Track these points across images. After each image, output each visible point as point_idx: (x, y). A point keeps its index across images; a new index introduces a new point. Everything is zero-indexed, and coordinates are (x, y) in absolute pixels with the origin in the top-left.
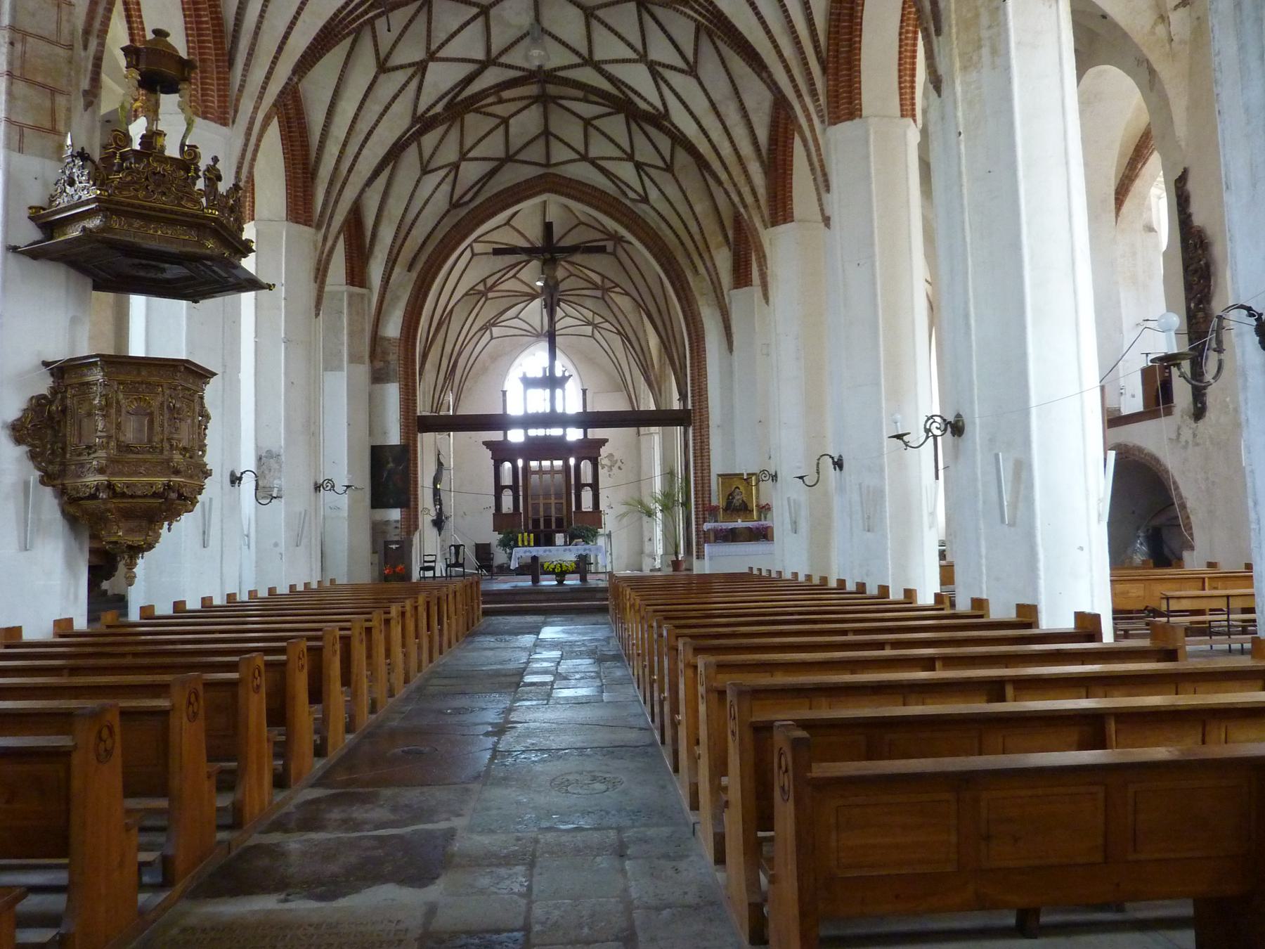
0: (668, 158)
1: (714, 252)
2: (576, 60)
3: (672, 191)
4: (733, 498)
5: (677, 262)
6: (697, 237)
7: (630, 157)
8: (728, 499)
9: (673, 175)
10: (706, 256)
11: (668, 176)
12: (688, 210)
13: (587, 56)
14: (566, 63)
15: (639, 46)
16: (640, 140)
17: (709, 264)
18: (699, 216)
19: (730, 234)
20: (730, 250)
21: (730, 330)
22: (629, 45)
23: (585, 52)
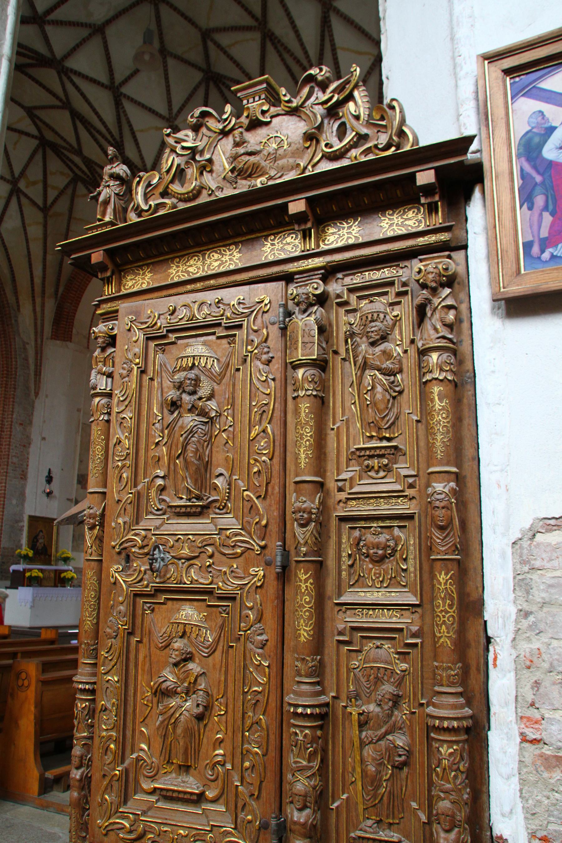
0: (50, 201)
1: (46, 300)
2: (104, 78)
3: (35, 231)
4: (37, 541)
5: (5, 294)
6: (38, 280)
7: (14, 182)
8: (33, 541)
9: (45, 217)
10: (38, 300)
11: (40, 216)
12: (41, 253)
13: (117, 84)
14: (92, 75)
15: (175, 109)
16: (35, 173)
17: (38, 309)
18: (48, 263)
19: (61, 290)
20: (56, 301)
21: (40, 375)
22: (170, 102)
23: (119, 78)
